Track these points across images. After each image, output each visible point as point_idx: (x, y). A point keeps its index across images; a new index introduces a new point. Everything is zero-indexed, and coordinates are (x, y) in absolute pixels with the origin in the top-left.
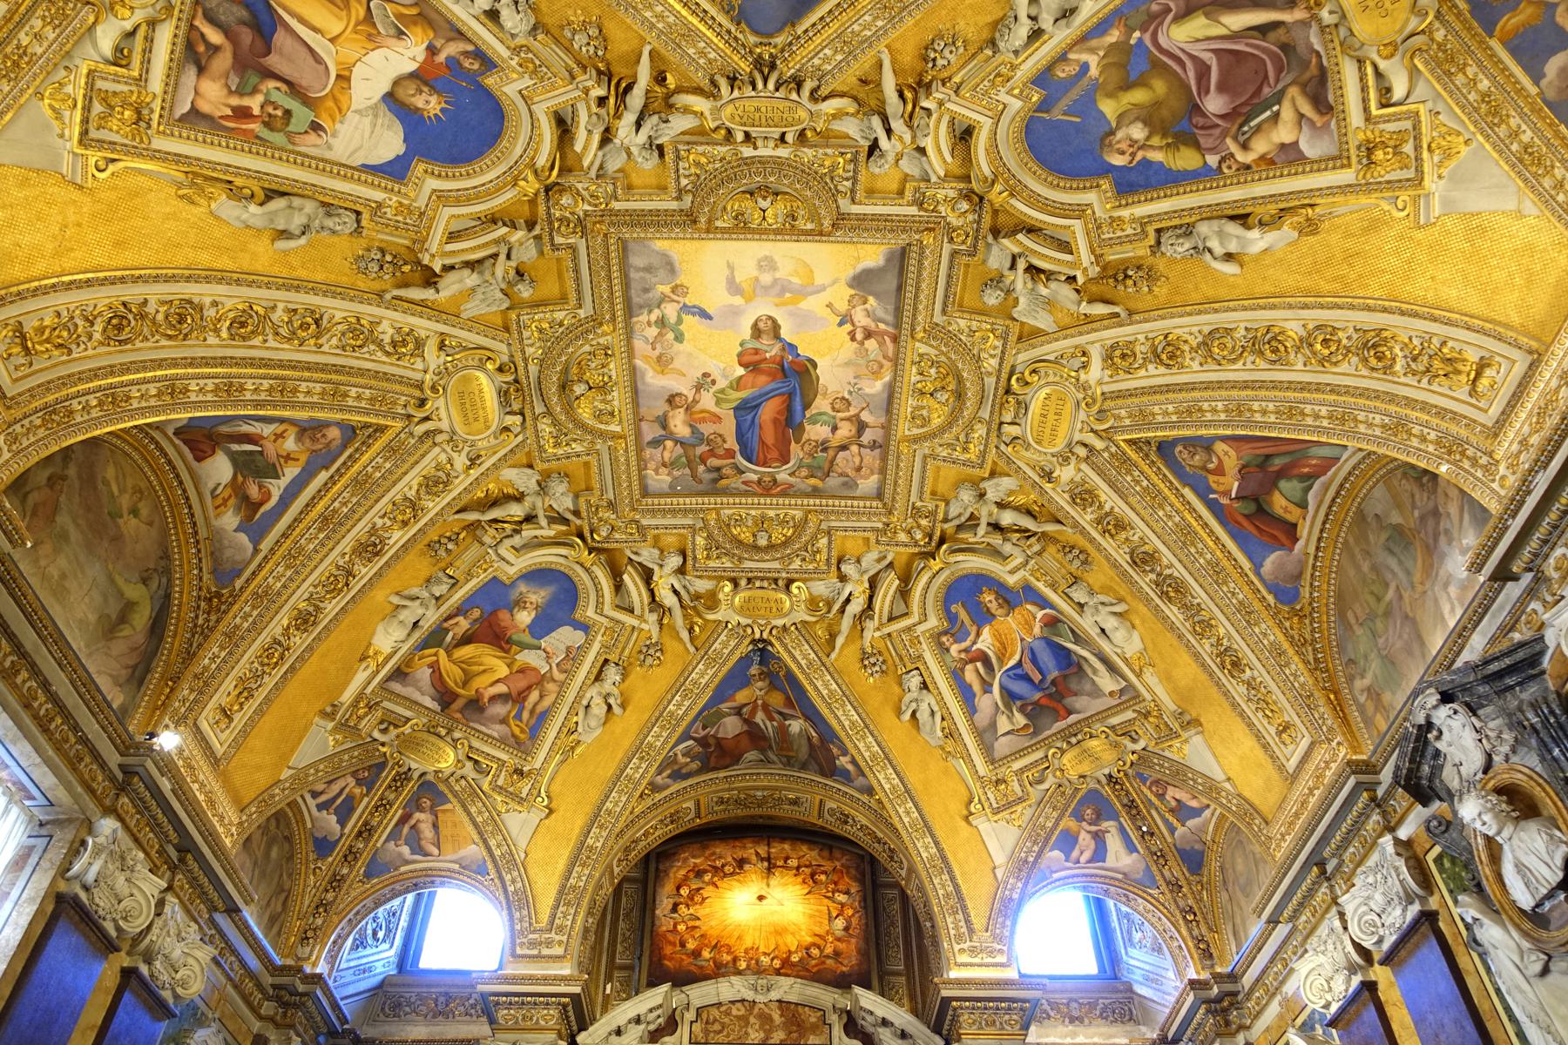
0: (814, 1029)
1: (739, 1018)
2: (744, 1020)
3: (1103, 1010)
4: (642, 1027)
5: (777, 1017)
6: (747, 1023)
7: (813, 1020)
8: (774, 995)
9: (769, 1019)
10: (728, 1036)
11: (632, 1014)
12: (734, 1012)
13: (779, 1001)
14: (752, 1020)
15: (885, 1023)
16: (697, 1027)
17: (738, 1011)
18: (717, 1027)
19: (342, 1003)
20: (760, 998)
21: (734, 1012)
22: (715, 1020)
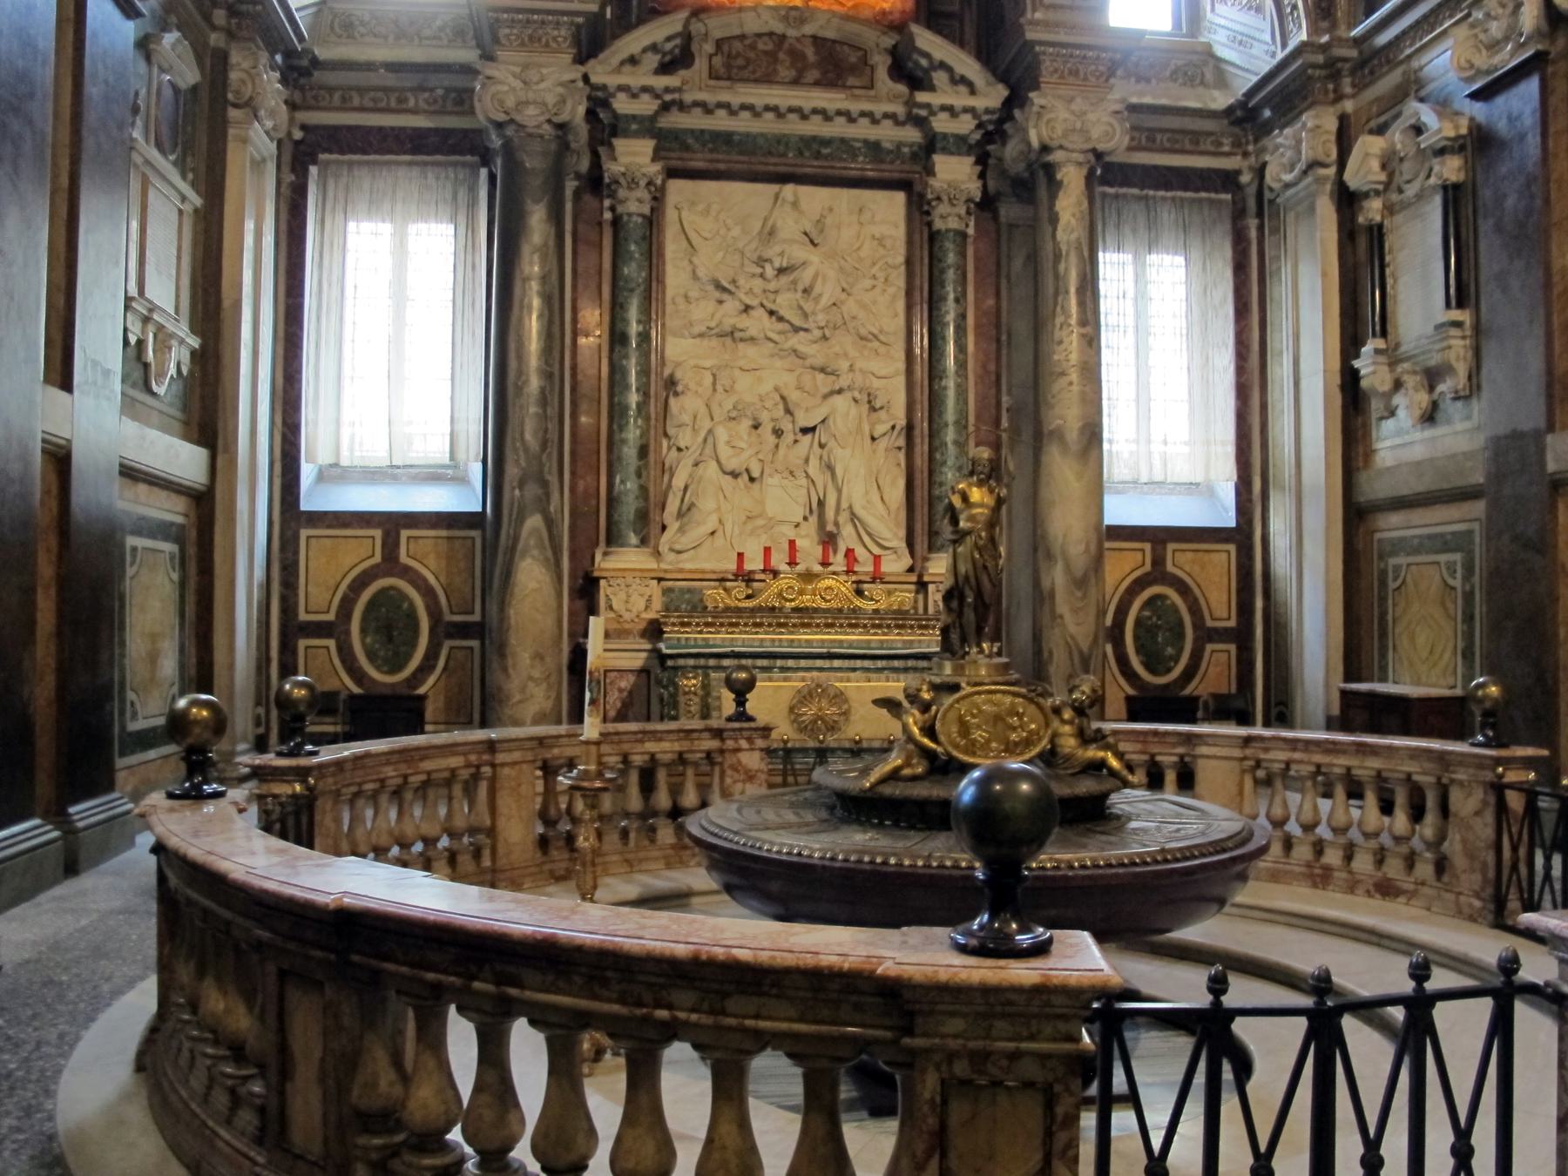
0: (854, 70)
1: (766, 53)
2: (772, 56)
3: (1174, 72)
4: (658, 57)
5: (810, 53)
6: (776, 60)
7: (853, 59)
8: (808, 29)
9: (803, 57)
10: (754, 72)
11: (646, 42)
12: (761, 46)
13: (815, 38)
14: (781, 56)
15: (943, 66)
16: (717, 61)
17: (765, 45)
18: (740, 62)
19: (297, 16)
20: (792, 33)
21: (761, 46)
22: (738, 55)
